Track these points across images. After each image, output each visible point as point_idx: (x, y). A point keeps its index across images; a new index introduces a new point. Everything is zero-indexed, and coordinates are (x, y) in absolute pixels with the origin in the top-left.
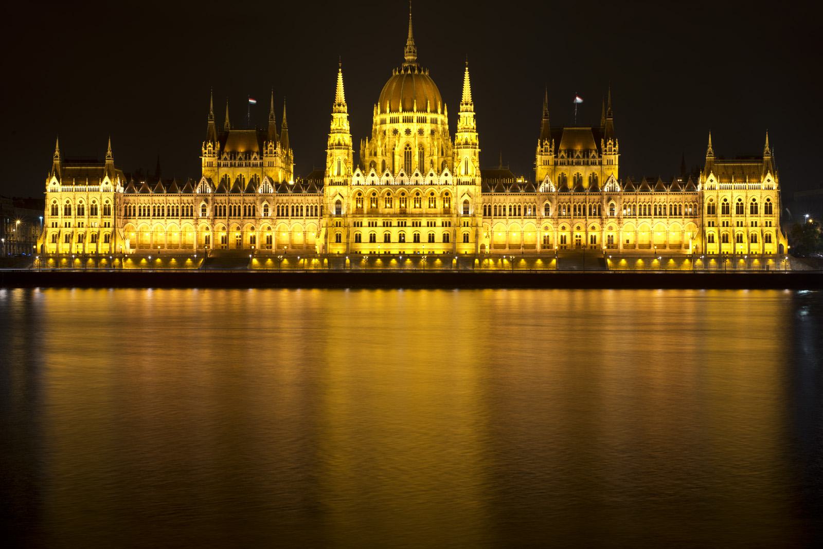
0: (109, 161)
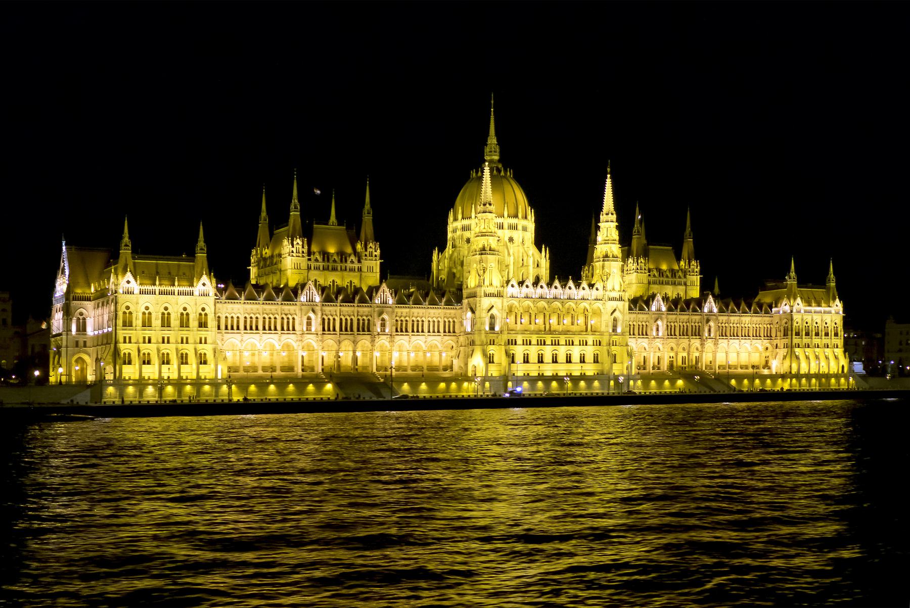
0: (201, 256)
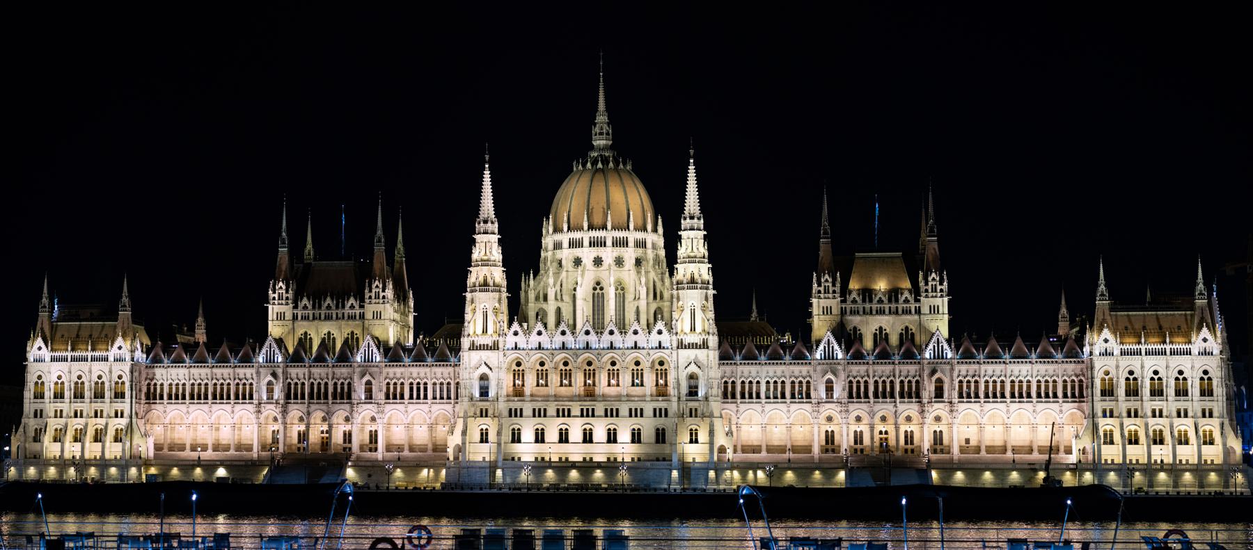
0: (125, 314)
